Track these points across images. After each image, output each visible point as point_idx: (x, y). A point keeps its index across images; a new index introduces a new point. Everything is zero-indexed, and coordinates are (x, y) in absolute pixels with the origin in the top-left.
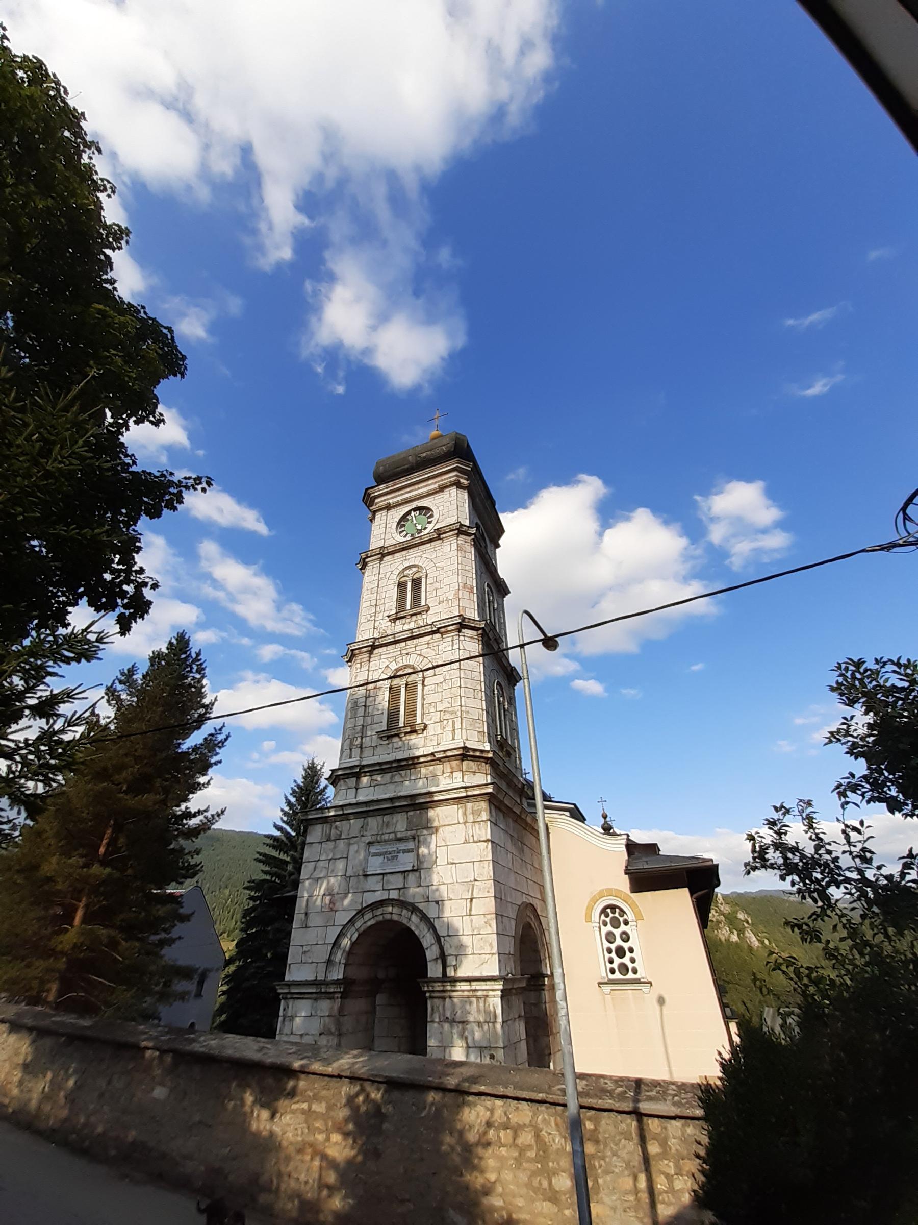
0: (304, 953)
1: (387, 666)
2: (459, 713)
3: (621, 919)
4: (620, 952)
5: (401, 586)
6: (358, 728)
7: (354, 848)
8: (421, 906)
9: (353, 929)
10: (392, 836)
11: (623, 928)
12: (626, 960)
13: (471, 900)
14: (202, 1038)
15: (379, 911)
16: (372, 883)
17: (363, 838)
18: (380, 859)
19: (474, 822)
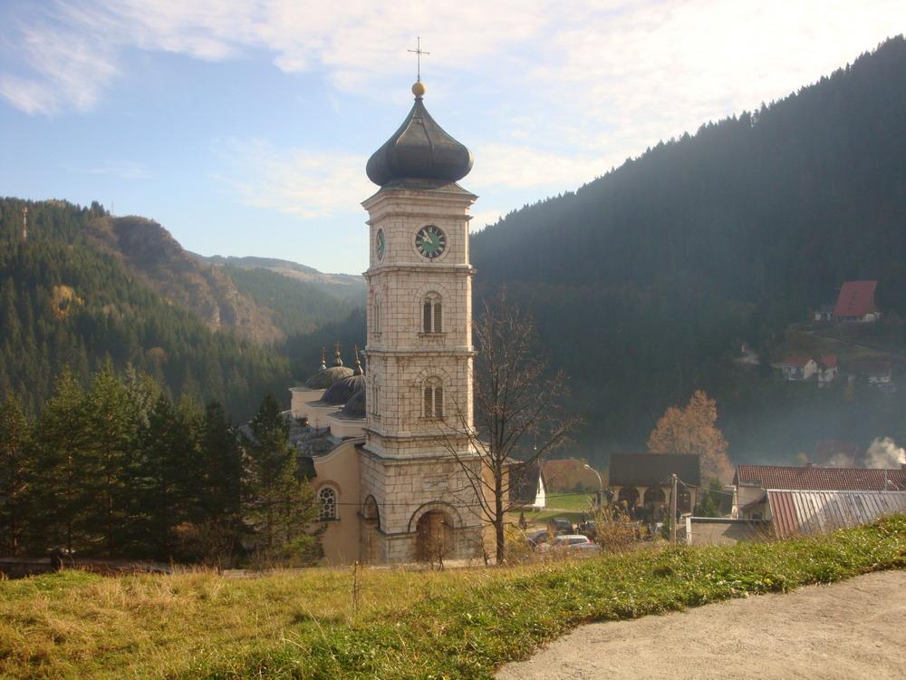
1: (421, 373)
5: (427, 306)
6: (407, 413)
18: (430, 485)
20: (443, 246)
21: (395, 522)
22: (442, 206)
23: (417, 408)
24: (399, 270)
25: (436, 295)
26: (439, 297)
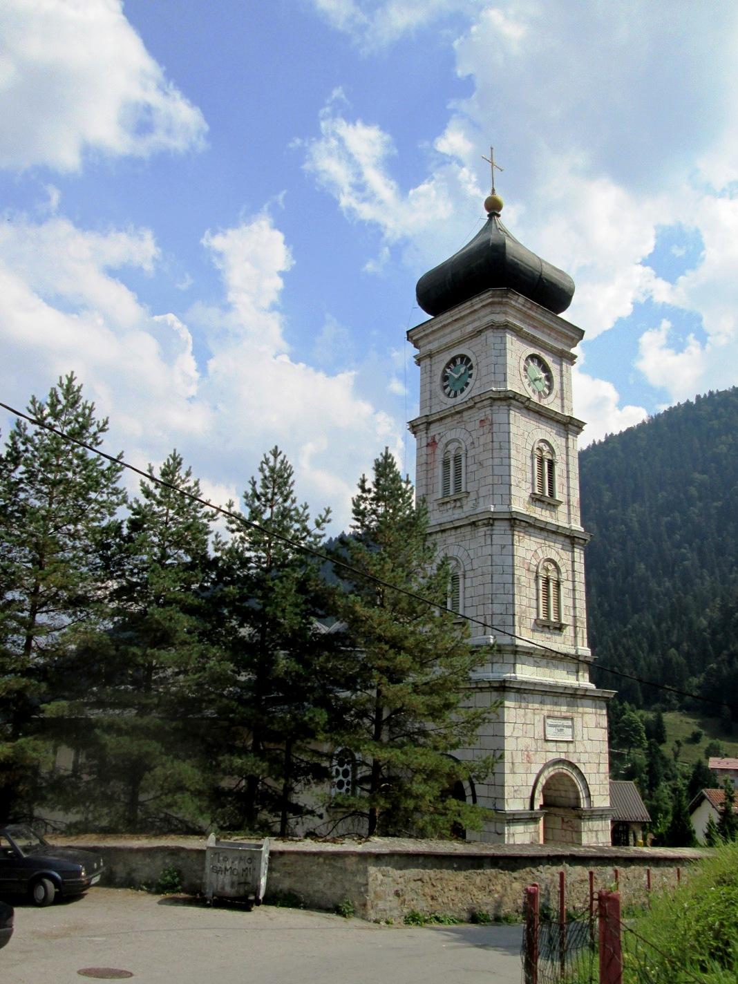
0: (515, 791)
7: (537, 717)
13: (599, 764)
15: (557, 767)
16: (551, 746)
20: (550, 388)
22: (549, 335)
24: (513, 398)
25: (548, 448)
26: (552, 451)
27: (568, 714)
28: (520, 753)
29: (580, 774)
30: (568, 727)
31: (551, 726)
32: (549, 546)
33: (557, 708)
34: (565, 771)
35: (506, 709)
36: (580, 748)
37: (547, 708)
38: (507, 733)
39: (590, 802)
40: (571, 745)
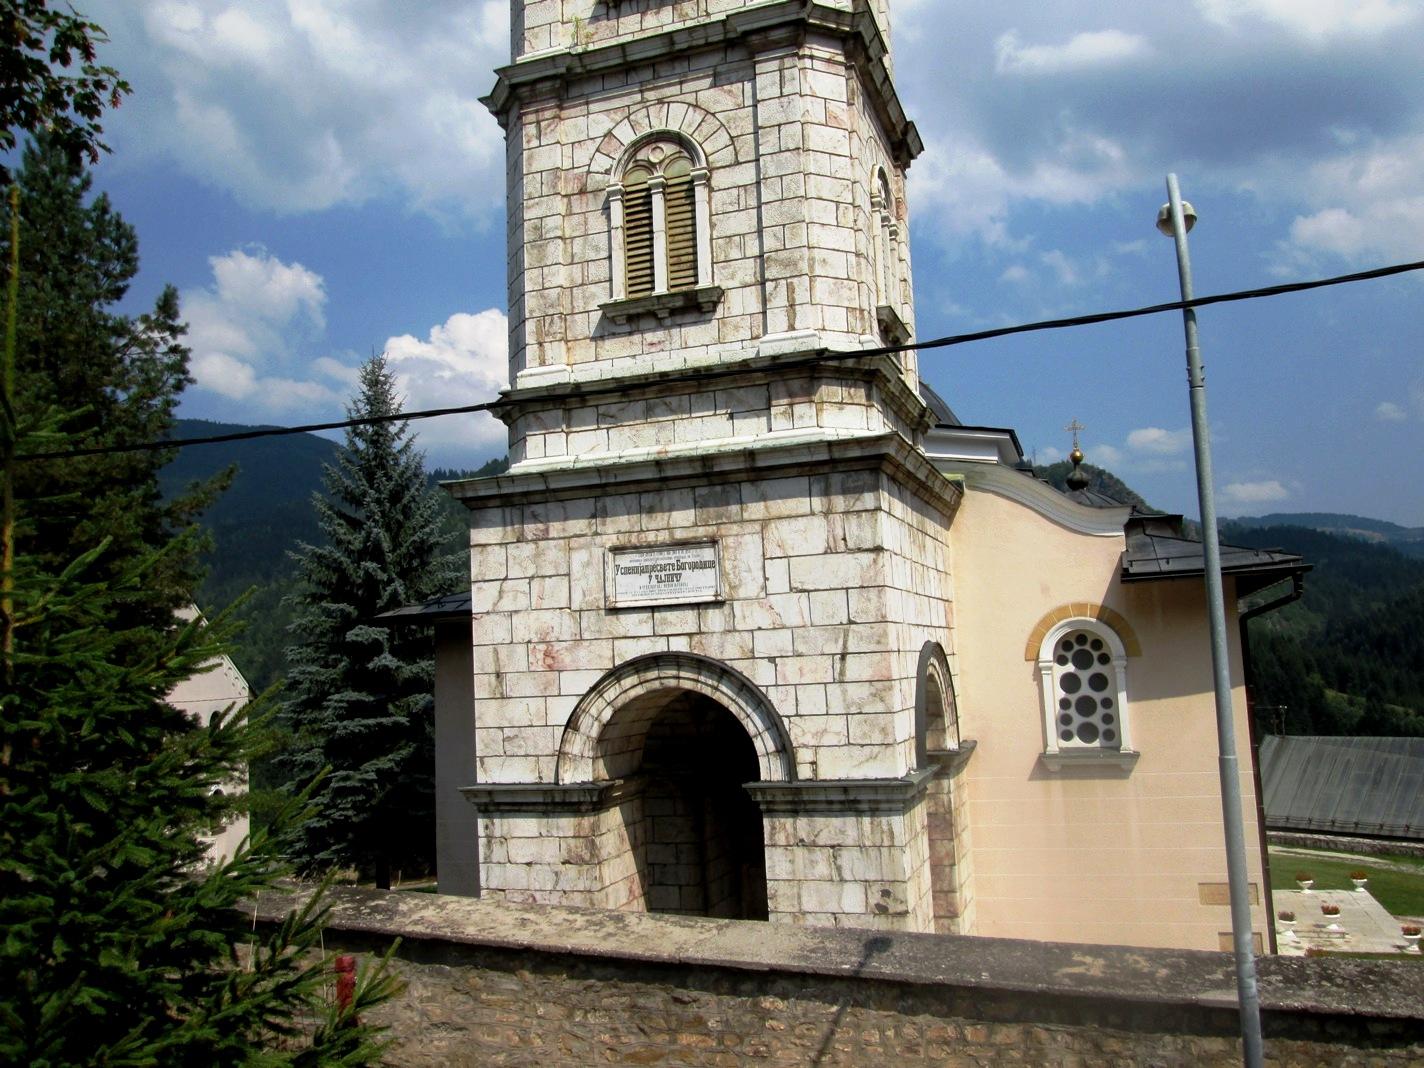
1: (609, 134)
2: (804, 267)
3: (1095, 654)
4: (1086, 706)
7: (579, 557)
8: (739, 666)
9: (600, 703)
10: (663, 537)
11: (1097, 668)
12: (1096, 719)
13: (843, 656)
14: (403, 907)
16: (629, 623)
17: (598, 539)
19: (846, 513)
21: (510, 735)
23: (598, 271)
27: (701, 532)
28: (521, 649)
29: (746, 688)
30: (703, 565)
31: (629, 571)
32: (660, 101)
33: (660, 520)
34: (687, 685)
35: (474, 552)
36: (749, 615)
37: (619, 526)
38: (477, 606)
39: (791, 765)
40: (715, 619)
